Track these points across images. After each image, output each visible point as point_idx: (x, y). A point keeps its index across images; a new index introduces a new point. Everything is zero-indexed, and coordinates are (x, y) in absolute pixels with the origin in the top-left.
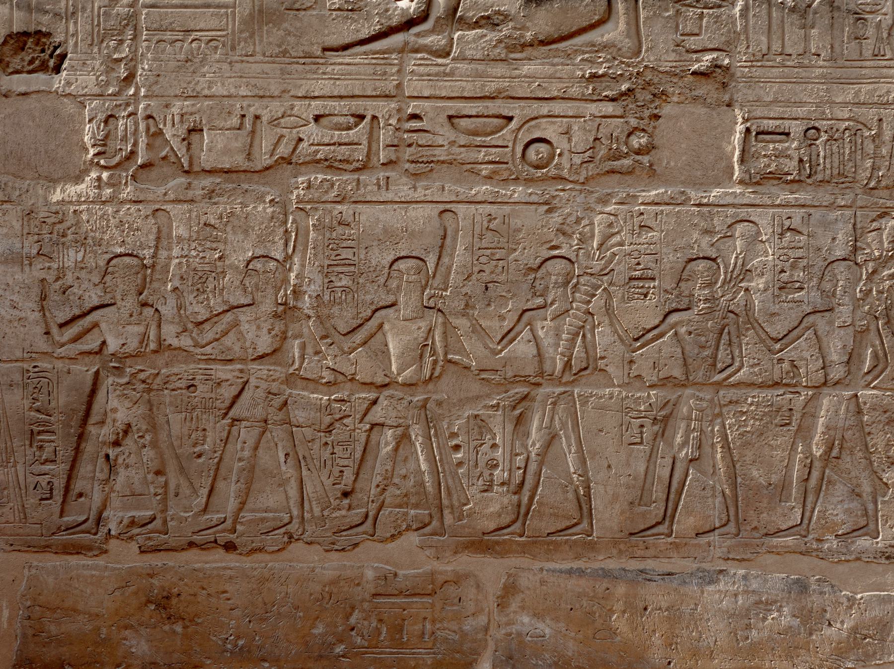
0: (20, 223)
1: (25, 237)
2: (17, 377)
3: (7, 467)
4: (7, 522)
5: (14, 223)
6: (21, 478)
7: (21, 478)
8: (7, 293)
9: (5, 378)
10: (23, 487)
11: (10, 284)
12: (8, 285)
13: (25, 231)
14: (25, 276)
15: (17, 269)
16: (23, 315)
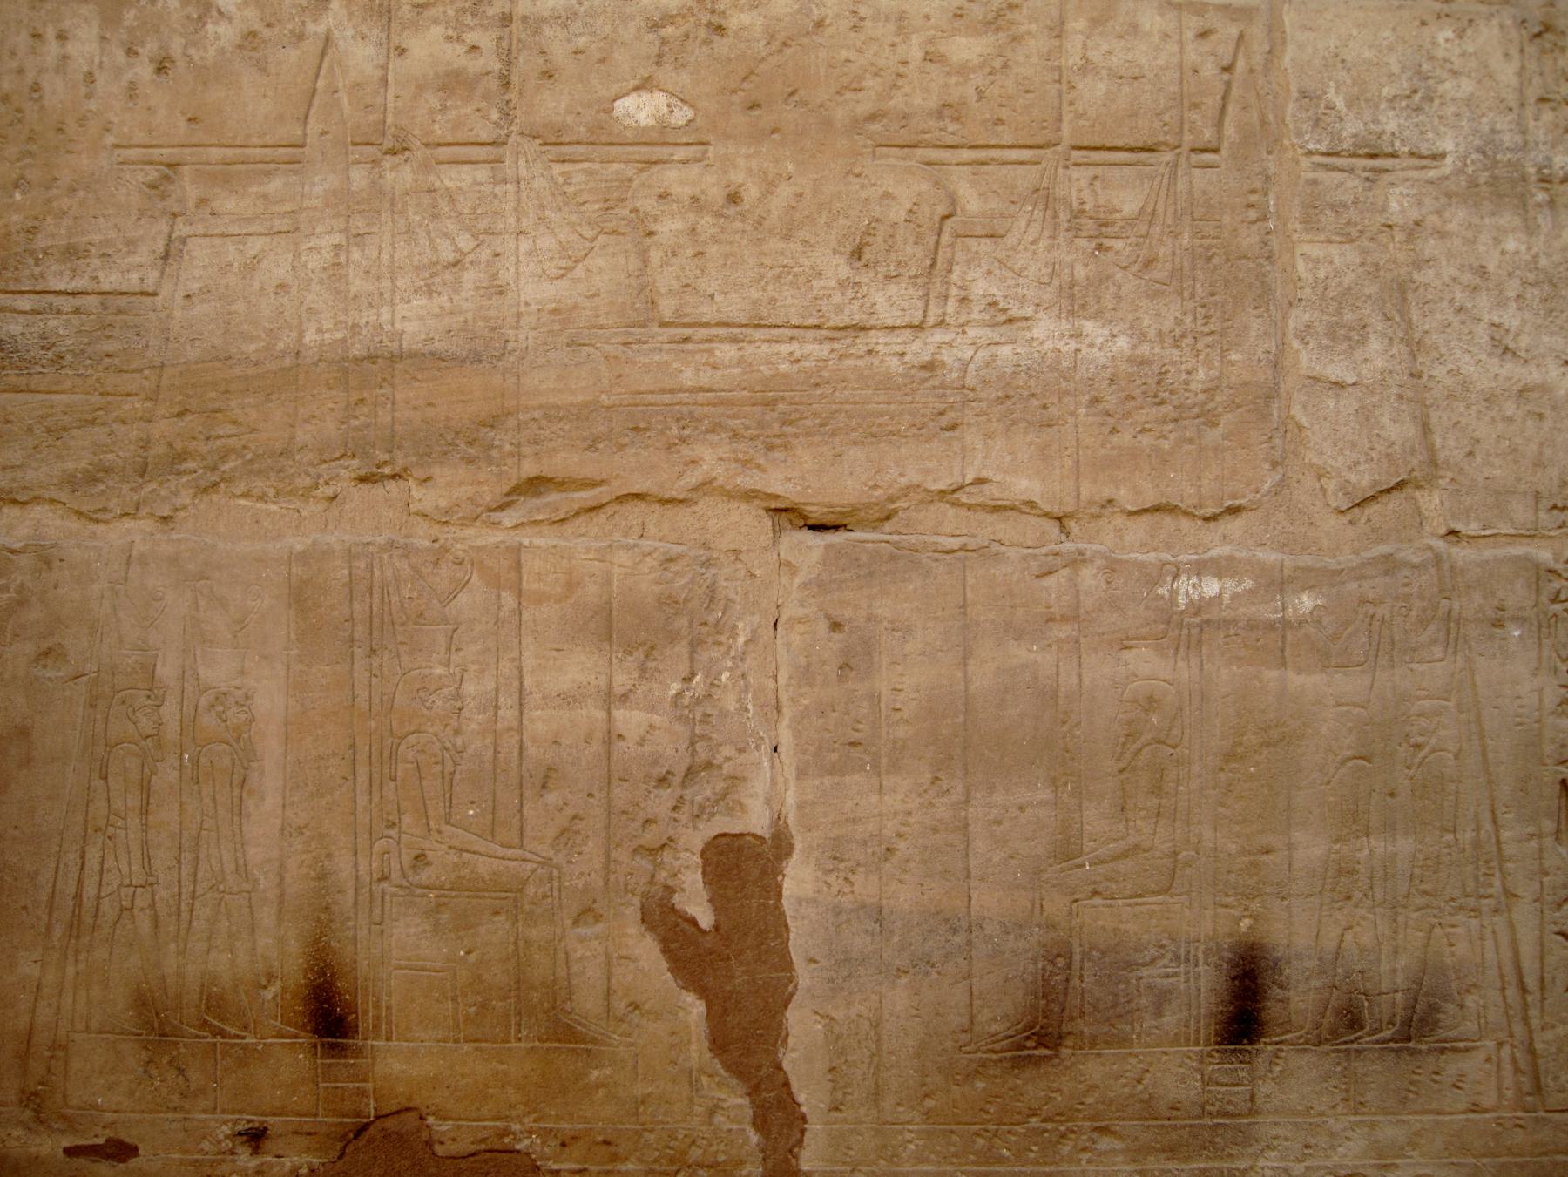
0: (1514, 66)
1: (1529, 111)
2: (1517, 595)
3: (1475, 912)
4: (1475, 1108)
5: (1496, 62)
6: (1528, 950)
7: (1528, 950)
8: (1483, 301)
9: (1477, 597)
10: (1531, 982)
11: (1491, 268)
12: (1482, 271)
13: (1533, 93)
14: (1539, 244)
15: (1507, 219)
16: (1533, 375)
